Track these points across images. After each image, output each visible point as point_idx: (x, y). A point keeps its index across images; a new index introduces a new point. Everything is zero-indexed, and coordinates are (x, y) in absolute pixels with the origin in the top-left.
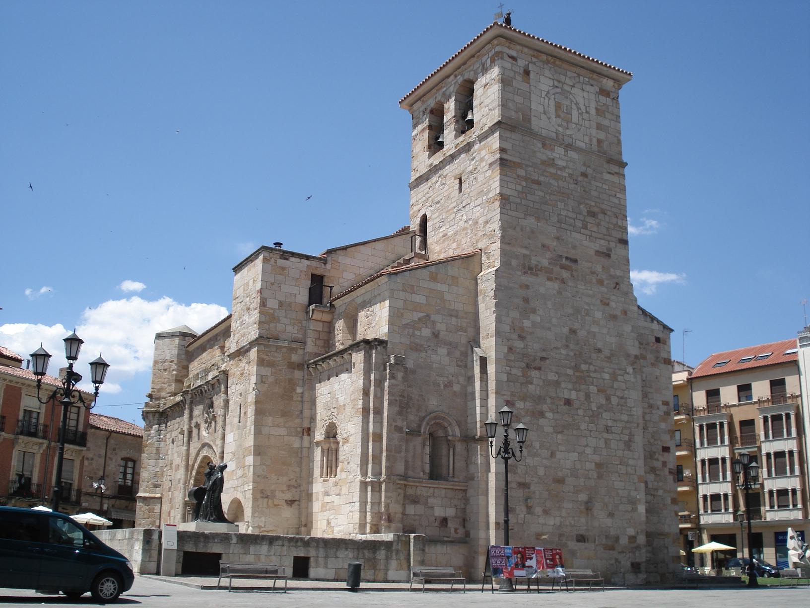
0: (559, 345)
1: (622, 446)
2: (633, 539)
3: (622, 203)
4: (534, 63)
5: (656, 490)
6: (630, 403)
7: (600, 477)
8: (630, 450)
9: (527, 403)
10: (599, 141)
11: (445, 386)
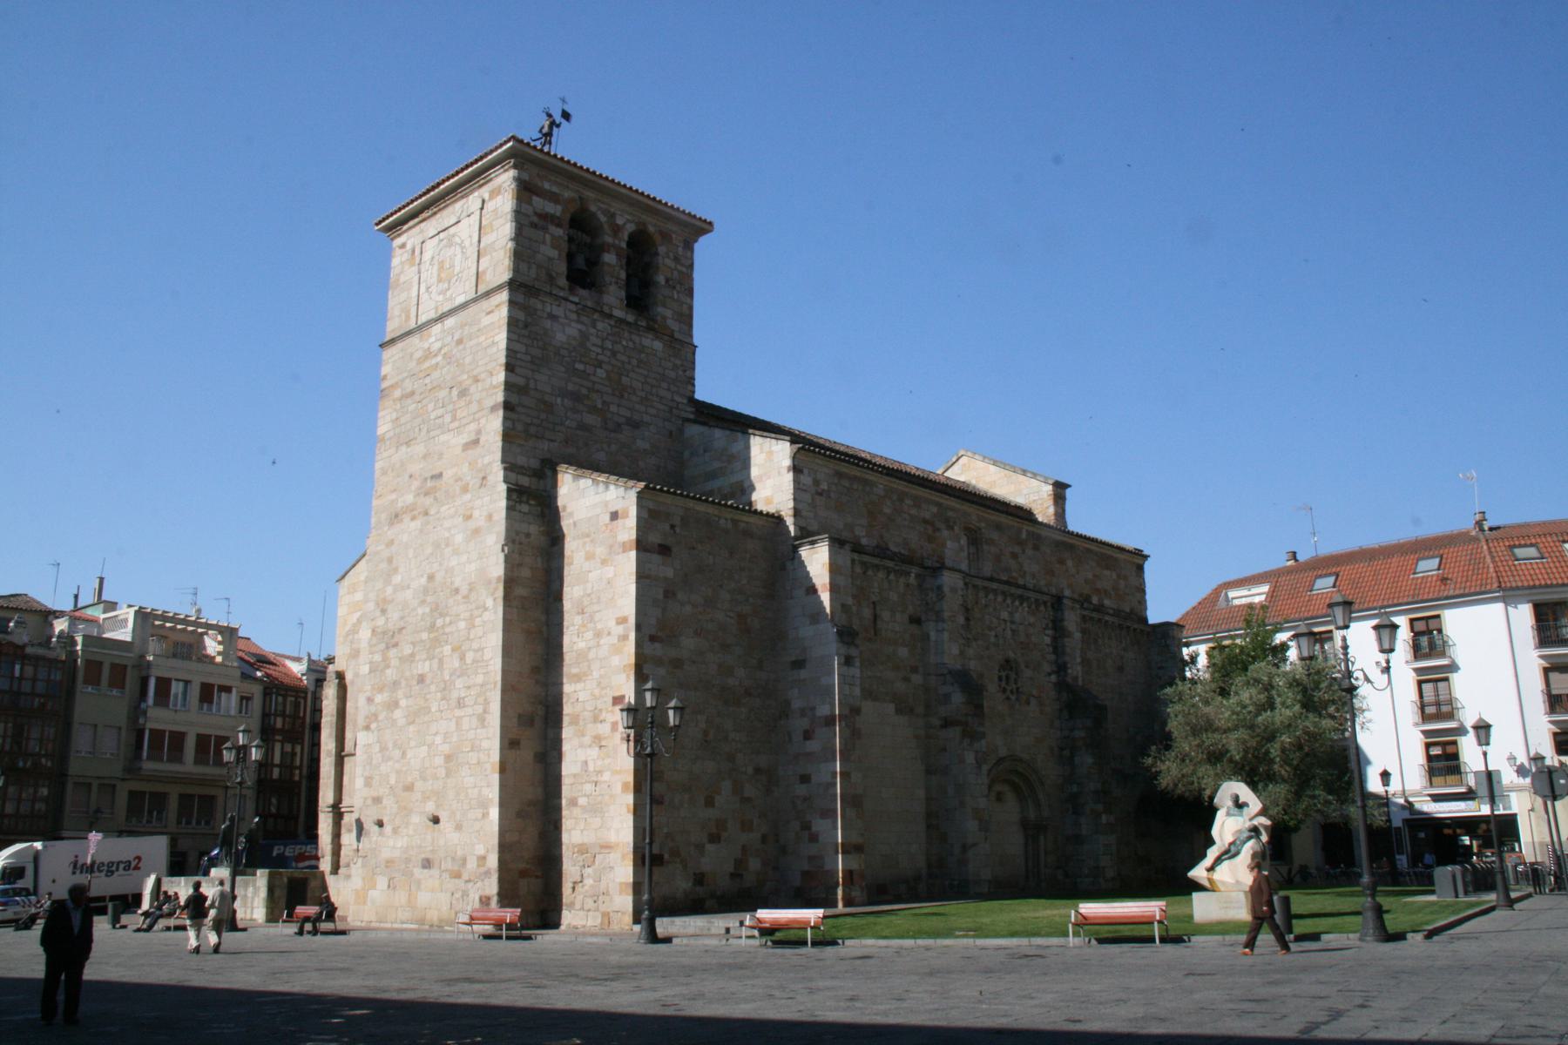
1: (475, 722)
5: (600, 772)
7: (448, 775)
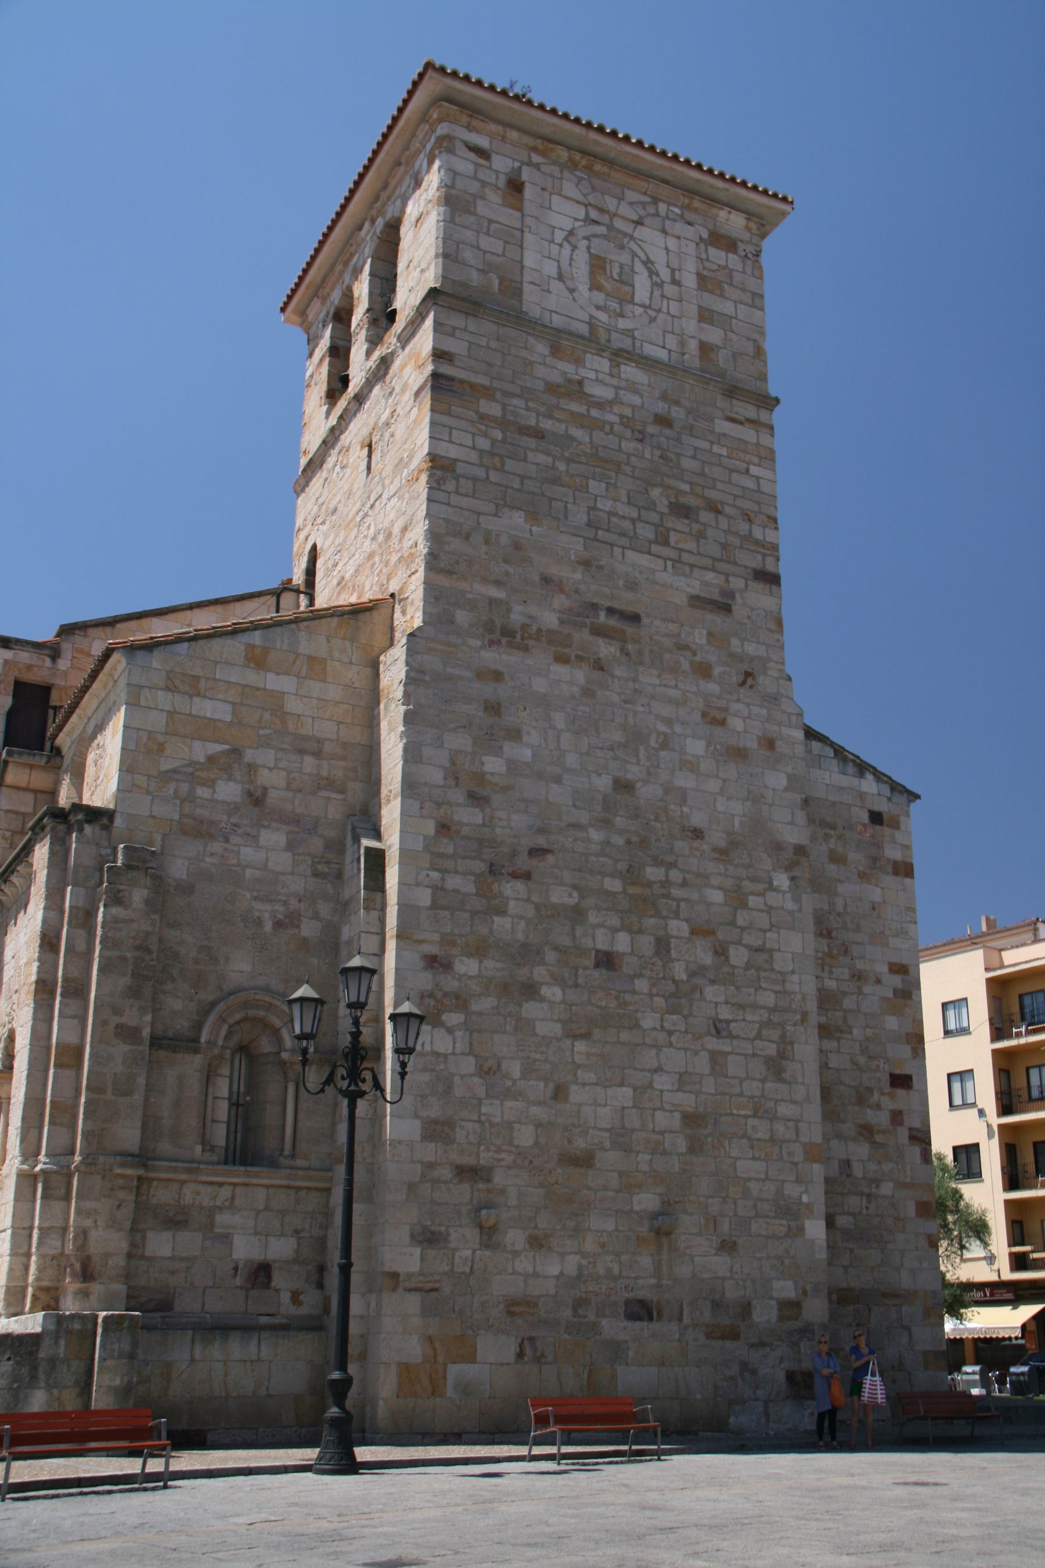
0: (584, 818)
2: (790, 1308)
3: (766, 487)
4: (537, 167)
5: (877, 1182)
6: (782, 962)
7: (695, 1148)
8: (781, 1080)
9: (489, 964)
10: (705, 349)
11: (278, 925)
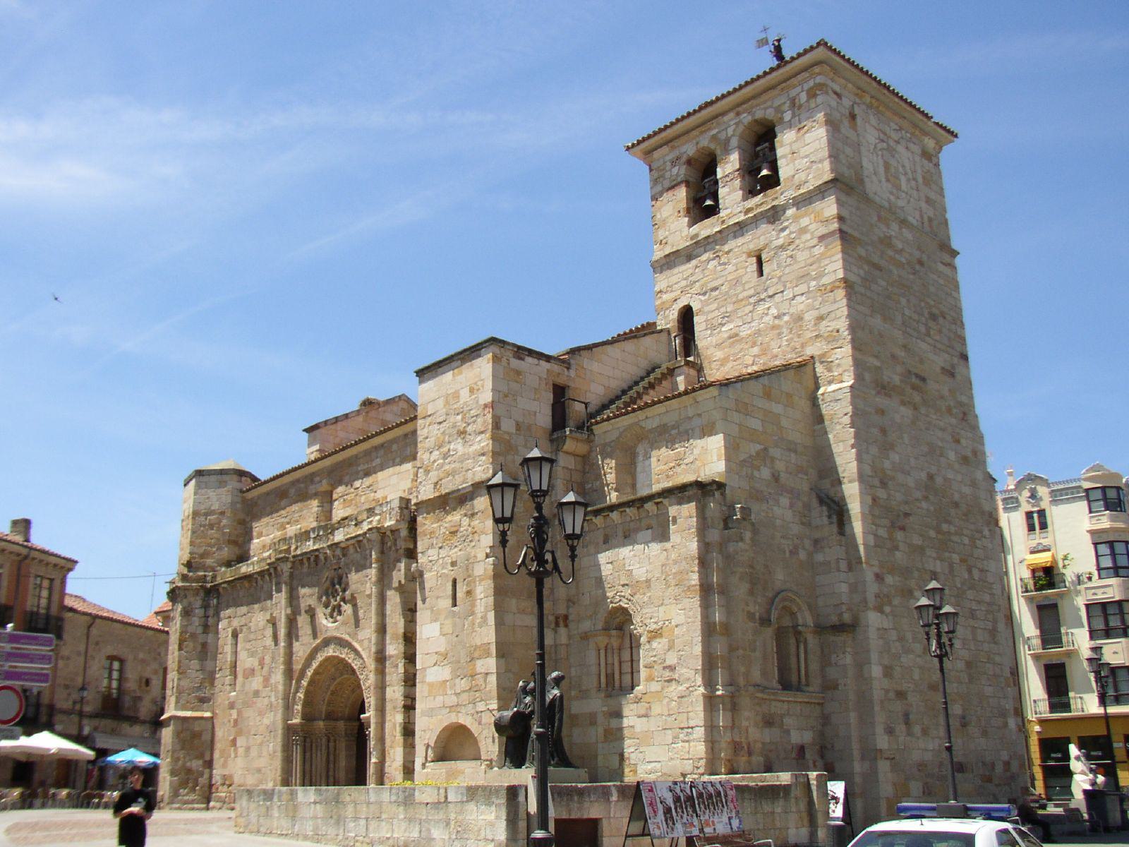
7: (971, 681)
